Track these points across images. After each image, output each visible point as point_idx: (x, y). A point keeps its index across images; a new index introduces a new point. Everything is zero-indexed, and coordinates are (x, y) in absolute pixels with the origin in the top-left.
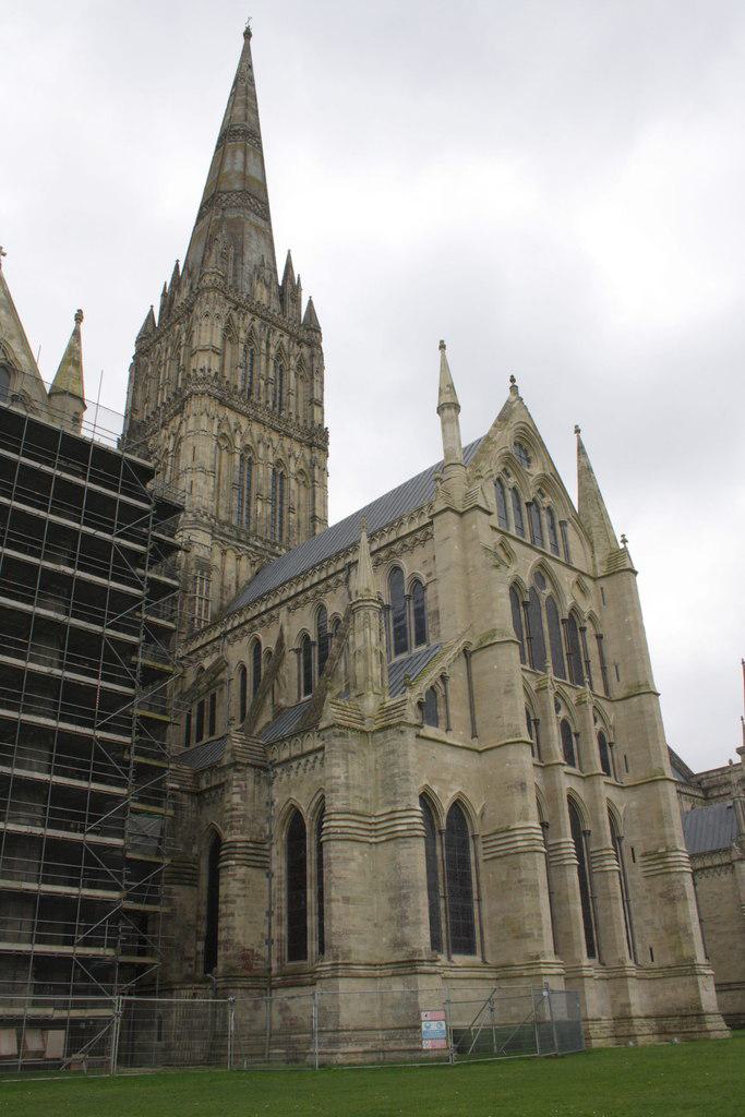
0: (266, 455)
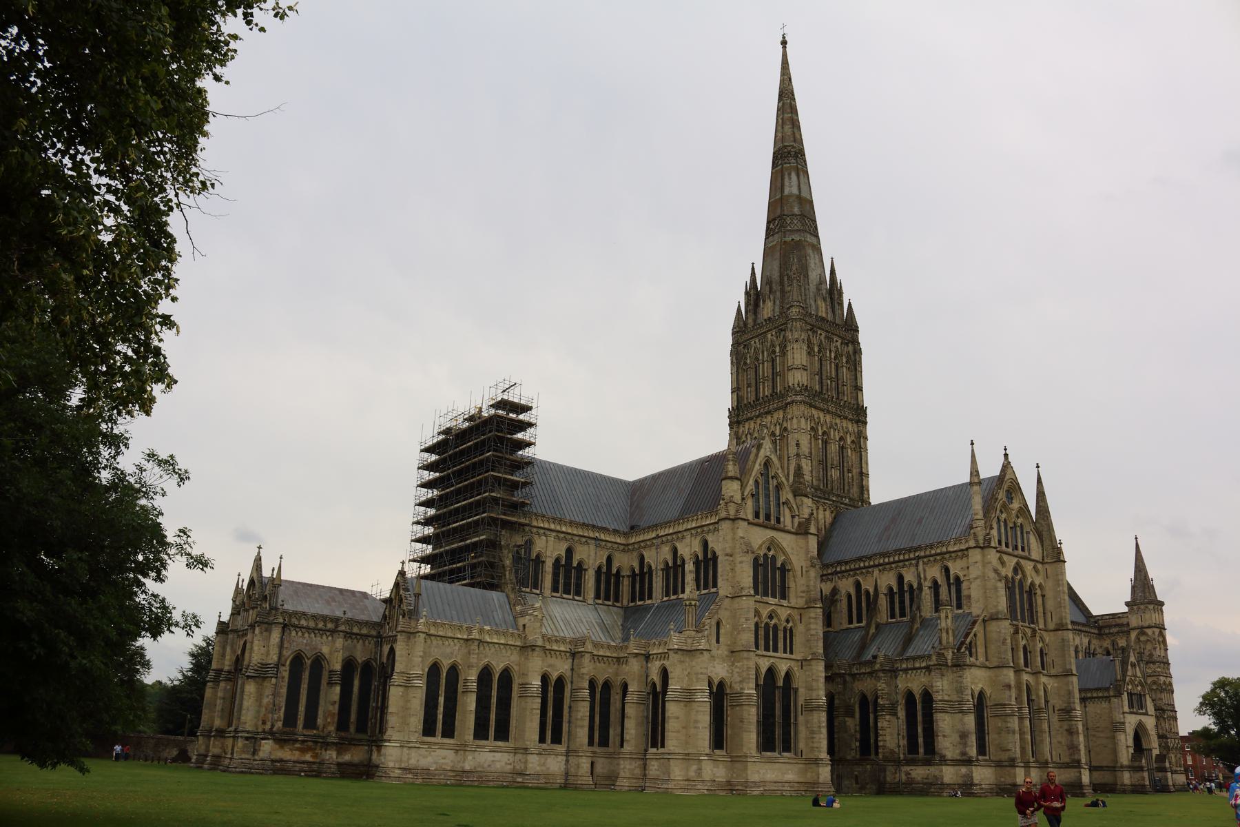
0: (834, 435)
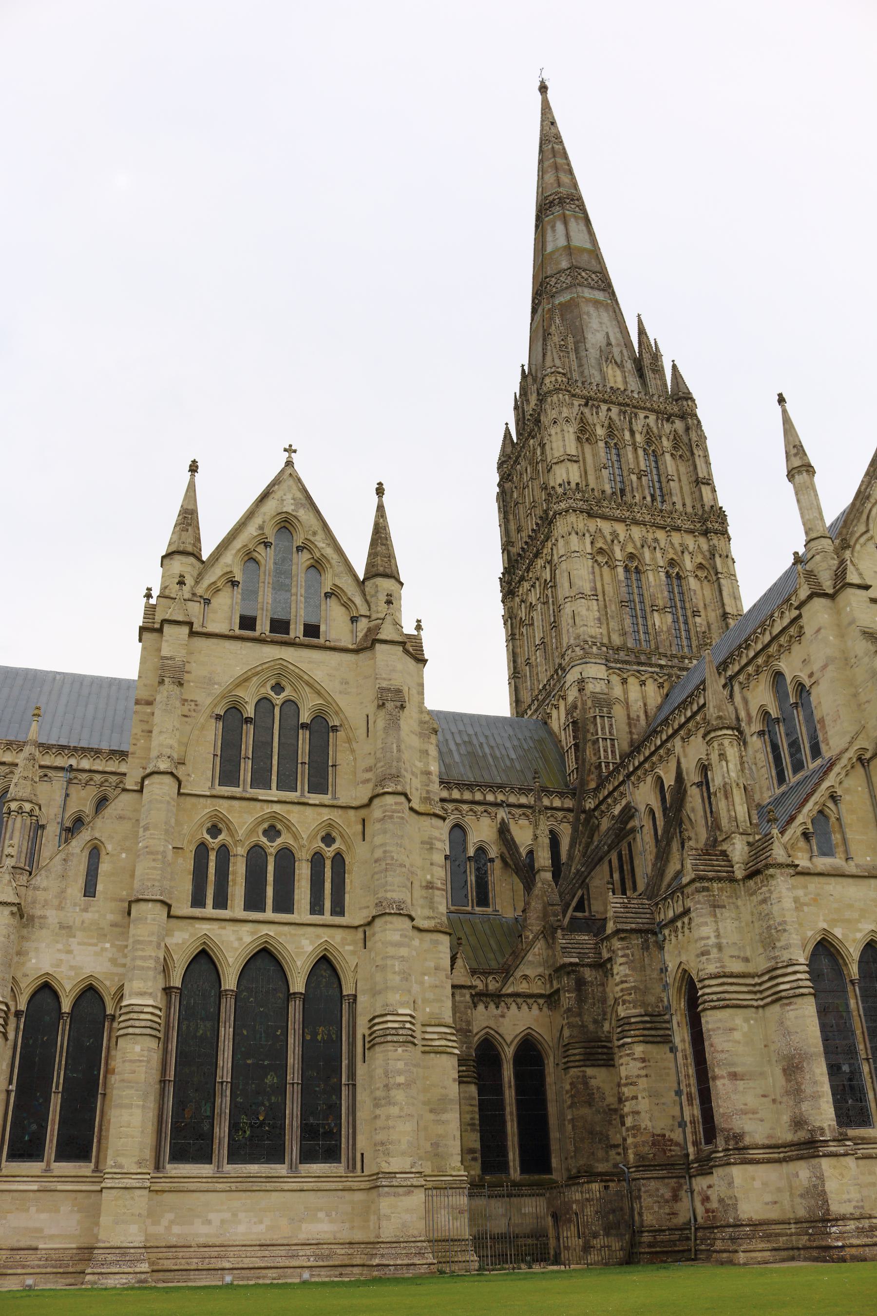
0: (654, 559)
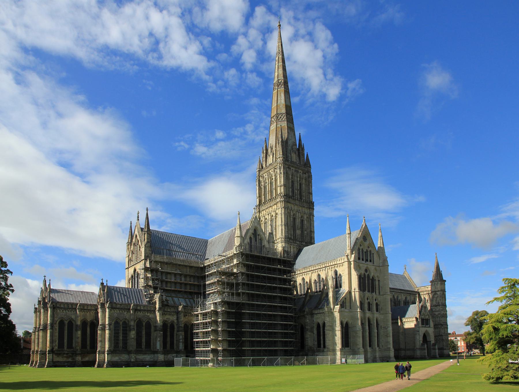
0: (299, 215)
